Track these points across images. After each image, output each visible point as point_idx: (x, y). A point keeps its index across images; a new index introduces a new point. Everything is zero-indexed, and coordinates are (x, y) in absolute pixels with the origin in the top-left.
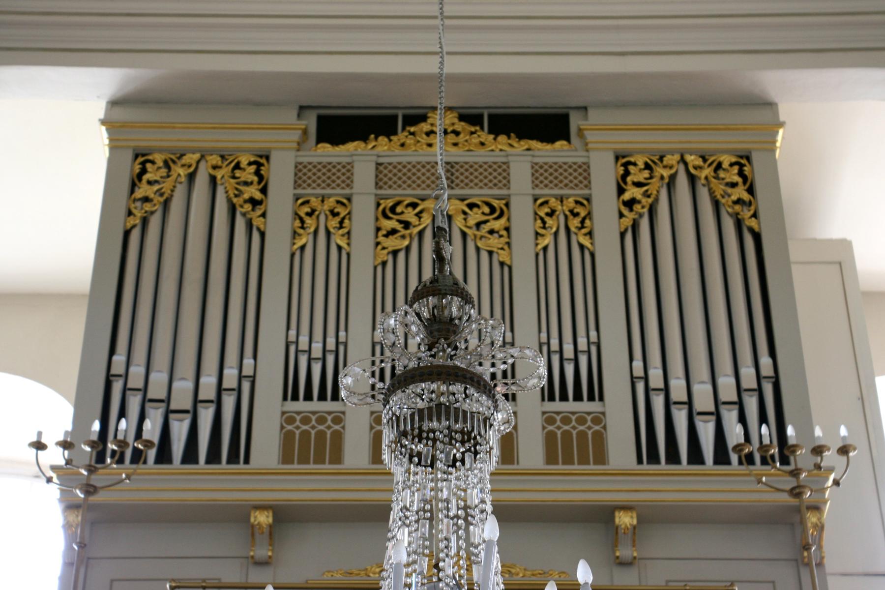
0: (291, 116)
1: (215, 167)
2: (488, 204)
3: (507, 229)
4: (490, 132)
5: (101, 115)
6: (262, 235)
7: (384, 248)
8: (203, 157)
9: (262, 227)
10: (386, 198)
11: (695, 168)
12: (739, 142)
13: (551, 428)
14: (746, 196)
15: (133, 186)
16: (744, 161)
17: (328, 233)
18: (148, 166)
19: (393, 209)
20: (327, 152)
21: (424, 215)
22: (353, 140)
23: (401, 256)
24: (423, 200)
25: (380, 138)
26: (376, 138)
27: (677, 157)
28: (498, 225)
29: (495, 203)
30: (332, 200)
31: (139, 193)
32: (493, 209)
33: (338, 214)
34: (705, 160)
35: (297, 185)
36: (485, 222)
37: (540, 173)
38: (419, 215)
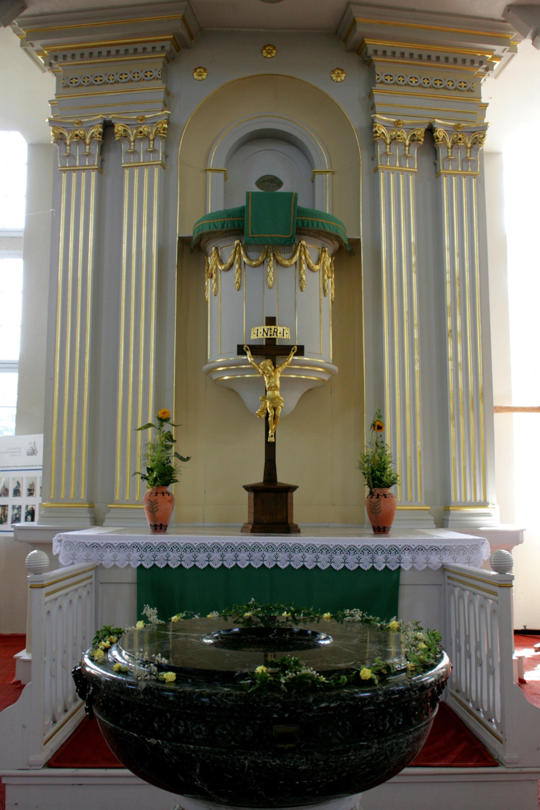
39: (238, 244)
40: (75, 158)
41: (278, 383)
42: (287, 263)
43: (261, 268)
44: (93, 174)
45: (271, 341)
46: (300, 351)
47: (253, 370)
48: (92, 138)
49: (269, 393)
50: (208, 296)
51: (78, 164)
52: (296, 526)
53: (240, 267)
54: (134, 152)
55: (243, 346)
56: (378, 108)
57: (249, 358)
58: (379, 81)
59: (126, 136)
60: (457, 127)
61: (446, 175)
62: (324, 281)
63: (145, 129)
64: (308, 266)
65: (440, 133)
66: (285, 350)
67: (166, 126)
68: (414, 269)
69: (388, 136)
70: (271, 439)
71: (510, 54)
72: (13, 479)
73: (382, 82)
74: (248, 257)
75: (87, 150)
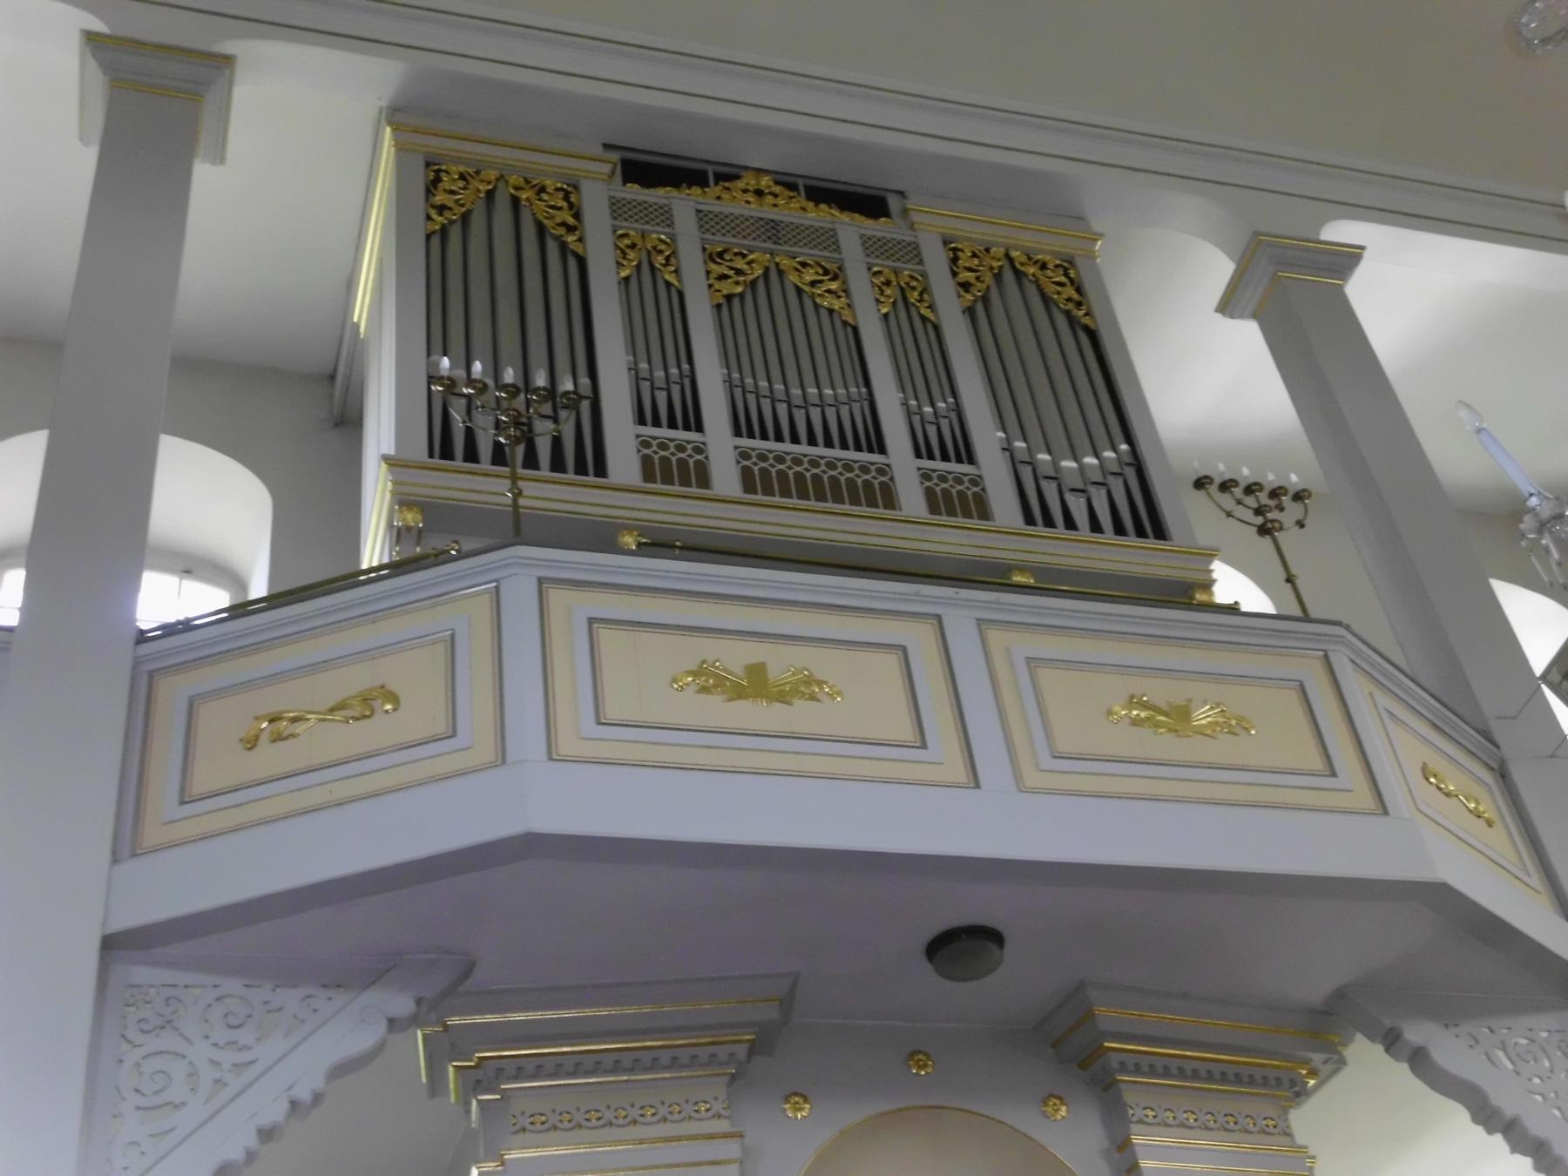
0: (598, 151)
2: (820, 265)
9: (580, 251)
10: (712, 243)
11: (1022, 264)
14: (1075, 296)
16: (1066, 264)
17: (652, 268)
19: (720, 255)
20: (634, 192)
23: (736, 302)
24: (751, 252)
27: (1002, 250)
28: (834, 286)
32: (826, 272)
33: (661, 252)
36: (821, 282)
37: (872, 246)
58: (1135, 1119)
71: (1336, 1066)
73: (1141, 1122)
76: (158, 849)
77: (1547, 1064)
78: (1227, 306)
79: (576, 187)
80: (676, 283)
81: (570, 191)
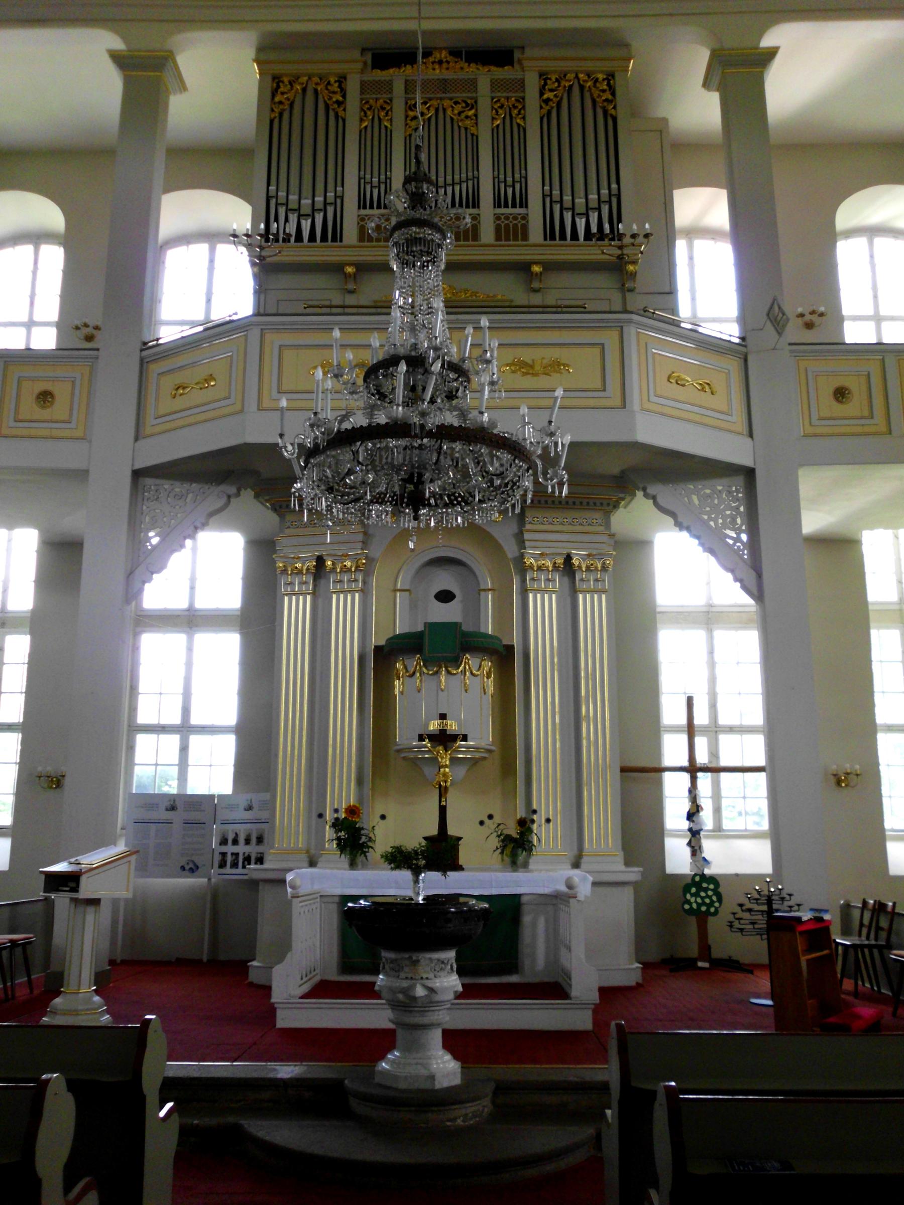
0: (356, 54)
1: (317, 84)
3: (476, 115)
4: (466, 61)
5: (254, 58)
6: (344, 120)
7: (410, 127)
8: (310, 78)
9: (343, 116)
12: (608, 66)
13: (498, 222)
15: (273, 95)
18: (281, 84)
21: (431, 109)
22: (392, 67)
25: (408, 66)
26: (405, 66)
28: (471, 113)
29: (469, 101)
30: (381, 101)
31: (277, 99)
32: (467, 105)
34: (589, 76)
35: (362, 93)
36: (463, 112)
37: (495, 85)
38: (428, 109)
39: (419, 658)
40: (294, 585)
41: (448, 763)
42: (455, 672)
43: (435, 677)
44: (309, 597)
45: (443, 732)
46: (465, 738)
47: (430, 751)
48: (308, 569)
49: (442, 770)
50: (397, 692)
51: (297, 589)
52: (461, 866)
53: (420, 674)
54: (341, 581)
55: (422, 735)
56: (527, 544)
57: (426, 742)
59: (333, 570)
60: (589, 555)
61: (581, 592)
62: (484, 682)
63: (348, 564)
64: (472, 673)
65: (575, 561)
66: (454, 738)
67: (364, 561)
68: (556, 667)
69: (535, 565)
70: (443, 803)
72: (232, 831)
74: (426, 668)
75: (304, 579)
76: (152, 435)
77: (716, 501)
78: (706, 84)
79: (345, 78)
80: (389, 126)
81: (342, 80)
